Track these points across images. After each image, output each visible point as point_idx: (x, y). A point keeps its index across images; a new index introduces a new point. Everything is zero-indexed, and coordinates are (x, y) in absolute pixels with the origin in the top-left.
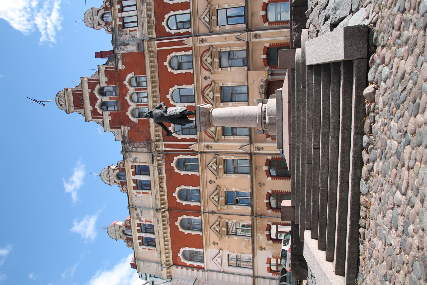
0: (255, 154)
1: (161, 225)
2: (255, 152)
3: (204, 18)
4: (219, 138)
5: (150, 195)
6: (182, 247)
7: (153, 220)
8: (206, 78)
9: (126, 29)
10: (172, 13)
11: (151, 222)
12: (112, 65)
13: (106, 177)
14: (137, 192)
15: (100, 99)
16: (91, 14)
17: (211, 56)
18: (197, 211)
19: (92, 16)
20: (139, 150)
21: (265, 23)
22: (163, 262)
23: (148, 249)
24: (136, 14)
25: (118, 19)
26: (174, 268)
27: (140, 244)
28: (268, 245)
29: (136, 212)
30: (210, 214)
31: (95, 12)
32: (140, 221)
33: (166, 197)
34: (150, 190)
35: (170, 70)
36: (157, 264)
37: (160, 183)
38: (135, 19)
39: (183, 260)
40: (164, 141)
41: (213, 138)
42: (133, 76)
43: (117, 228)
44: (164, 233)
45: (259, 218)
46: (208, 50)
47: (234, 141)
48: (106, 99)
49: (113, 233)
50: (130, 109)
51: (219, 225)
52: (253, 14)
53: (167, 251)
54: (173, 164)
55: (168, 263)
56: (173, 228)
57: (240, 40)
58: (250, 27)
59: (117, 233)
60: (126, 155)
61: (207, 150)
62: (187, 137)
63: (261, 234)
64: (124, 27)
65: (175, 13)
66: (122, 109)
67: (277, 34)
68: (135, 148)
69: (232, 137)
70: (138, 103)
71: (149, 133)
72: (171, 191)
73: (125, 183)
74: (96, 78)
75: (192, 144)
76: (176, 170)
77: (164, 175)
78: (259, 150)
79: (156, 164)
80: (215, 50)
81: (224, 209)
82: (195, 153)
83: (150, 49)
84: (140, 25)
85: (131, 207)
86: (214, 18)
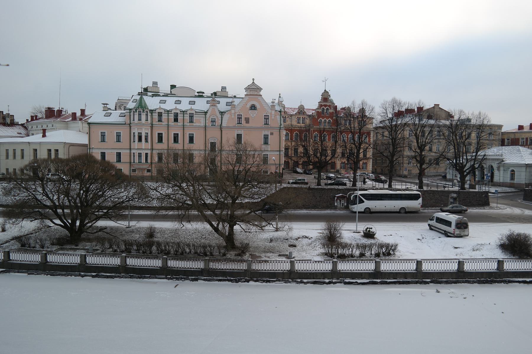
1: (287, 126)
8: (329, 145)
10: (346, 136)
15: (325, 108)
33: (295, 129)
34: (298, 123)
48: (325, 111)
73: (299, 114)
85: (291, 115)
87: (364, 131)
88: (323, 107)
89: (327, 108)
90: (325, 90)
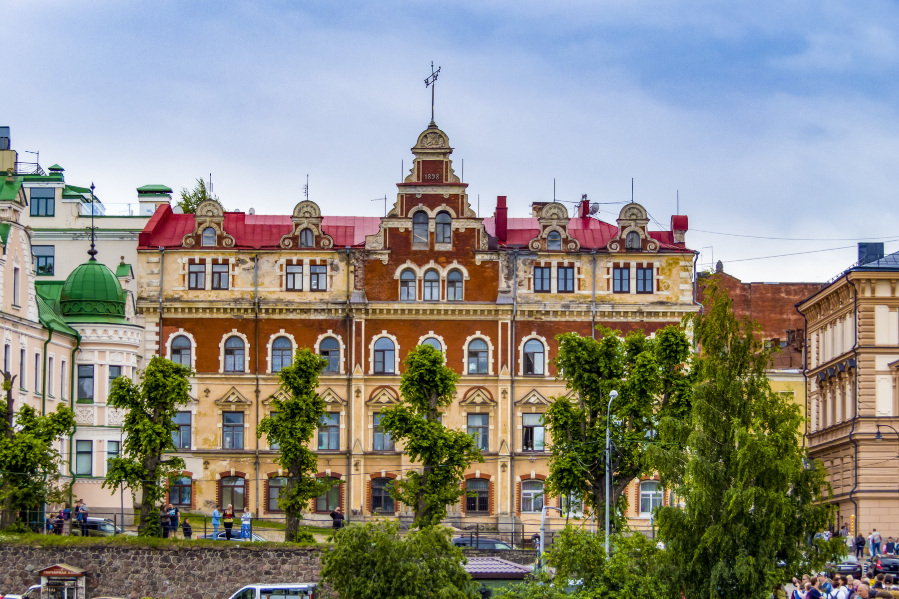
0: (349, 458)
1: (232, 306)
2: (353, 460)
3: (534, 395)
4: (371, 408)
5: (278, 289)
6: (195, 337)
7: (236, 289)
9: (532, 273)
10: (547, 348)
11: (233, 286)
12: (484, 243)
13: (305, 209)
14: (281, 265)
16: (560, 215)
17: (484, 403)
18: (258, 366)
19: (558, 219)
20: (352, 276)
21: (521, 477)
22: (168, 305)
23: (184, 275)
24: (552, 292)
25: (548, 260)
26: (157, 320)
27: (192, 262)
28: (212, 474)
29: (248, 260)
30: (254, 388)
31: (563, 222)
32: (233, 265)
33: (277, 316)
34: (288, 290)
35: (469, 339)
36: (159, 288)
37: (300, 309)
38: (546, 288)
39: (172, 336)
40: (366, 320)
41: (371, 399)
42: (464, 279)
43: (216, 220)
44: (218, 309)
45: (254, 461)
46: (492, 400)
47: (366, 430)
48: (432, 227)
49: (205, 209)
50: (413, 266)
51: (239, 401)
52: (532, 461)
53: (187, 311)
54: (330, 333)
55: (165, 310)
56: (226, 325)
57: (502, 444)
58: (516, 458)
59: (208, 219)
60: (343, 252)
61: (354, 389)
62: (371, 359)
63: (229, 464)
64: (535, 267)
65: (547, 353)
66: (416, 252)
67: (504, 493)
68: (355, 270)
69: (371, 426)
70: (423, 282)
71: (378, 299)
72: (289, 325)
74: (466, 210)
75: (361, 366)
76: (321, 337)
77: (313, 316)
78: (356, 465)
79: (330, 306)
80: (491, 408)
81: (265, 409)
82: (348, 370)
83: (500, 313)
84: (537, 296)
86: (534, 409)
87: (645, 319)
88: (421, 206)
89: (438, 209)
90: (433, 126)
